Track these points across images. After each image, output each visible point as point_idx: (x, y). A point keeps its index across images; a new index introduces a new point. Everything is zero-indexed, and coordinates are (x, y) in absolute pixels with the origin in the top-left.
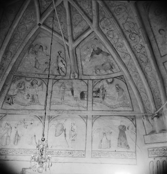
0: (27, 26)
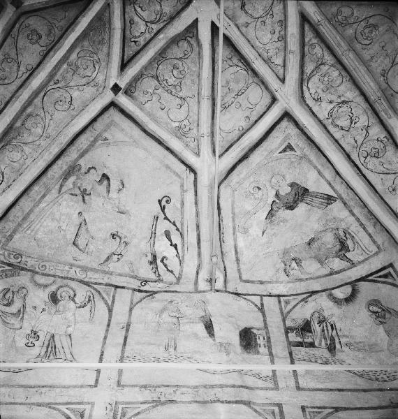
0: (75, 94)
